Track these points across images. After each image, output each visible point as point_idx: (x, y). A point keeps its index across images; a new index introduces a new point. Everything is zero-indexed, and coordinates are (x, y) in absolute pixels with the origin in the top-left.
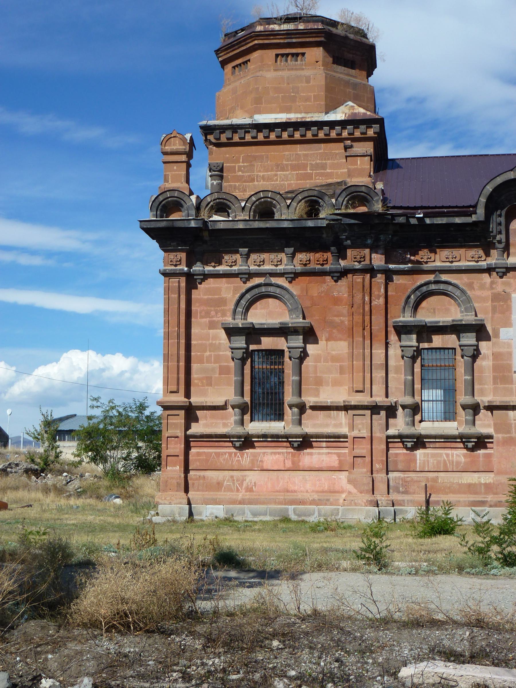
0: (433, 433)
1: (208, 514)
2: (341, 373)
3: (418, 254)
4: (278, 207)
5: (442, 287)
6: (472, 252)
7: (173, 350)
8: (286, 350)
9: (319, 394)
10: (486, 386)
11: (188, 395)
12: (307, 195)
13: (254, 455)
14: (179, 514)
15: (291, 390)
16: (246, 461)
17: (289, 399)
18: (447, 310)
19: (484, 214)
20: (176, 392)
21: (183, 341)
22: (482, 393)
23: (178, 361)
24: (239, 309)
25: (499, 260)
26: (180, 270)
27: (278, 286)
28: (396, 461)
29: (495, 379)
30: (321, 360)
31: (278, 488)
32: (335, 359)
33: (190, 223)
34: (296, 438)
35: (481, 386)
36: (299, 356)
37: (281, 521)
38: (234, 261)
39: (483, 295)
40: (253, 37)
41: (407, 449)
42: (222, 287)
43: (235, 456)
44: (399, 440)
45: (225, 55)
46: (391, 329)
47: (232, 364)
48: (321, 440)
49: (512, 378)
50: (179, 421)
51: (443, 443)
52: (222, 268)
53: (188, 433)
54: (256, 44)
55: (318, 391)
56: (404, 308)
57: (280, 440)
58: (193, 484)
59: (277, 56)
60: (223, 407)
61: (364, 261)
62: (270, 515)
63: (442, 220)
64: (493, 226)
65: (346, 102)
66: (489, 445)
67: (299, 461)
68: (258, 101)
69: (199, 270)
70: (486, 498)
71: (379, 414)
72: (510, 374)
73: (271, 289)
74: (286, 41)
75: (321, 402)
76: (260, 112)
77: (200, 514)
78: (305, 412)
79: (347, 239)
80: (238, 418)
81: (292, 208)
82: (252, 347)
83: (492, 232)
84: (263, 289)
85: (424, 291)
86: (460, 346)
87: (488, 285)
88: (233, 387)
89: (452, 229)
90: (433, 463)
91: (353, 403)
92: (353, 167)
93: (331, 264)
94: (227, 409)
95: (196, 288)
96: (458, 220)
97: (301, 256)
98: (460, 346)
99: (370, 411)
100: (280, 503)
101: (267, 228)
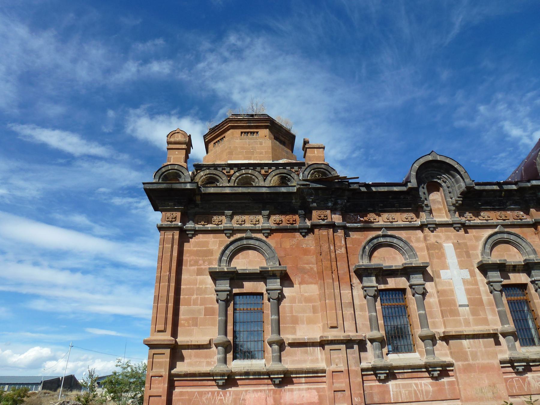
0: (402, 364)
3: (367, 216)
4: (257, 180)
5: (388, 239)
6: (405, 215)
7: (164, 293)
8: (265, 292)
9: (295, 332)
10: (437, 320)
11: (174, 334)
12: (279, 172)
13: (236, 393)
15: (270, 329)
16: (228, 400)
17: (269, 337)
18: (394, 258)
19: (416, 183)
20: (164, 331)
21: (173, 285)
22: (435, 325)
23: (167, 303)
24: (224, 258)
26: (175, 224)
28: (372, 393)
30: (296, 300)
32: (308, 300)
33: (186, 186)
34: (278, 374)
35: (433, 320)
36: (277, 297)
38: (220, 220)
39: (420, 247)
40: (228, 122)
41: (380, 380)
42: (210, 241)
43: (218, 395)
44: (372, 373)
45: (210, 137)
46: (353, 274)
47: (217, 306)
48: (301, 375)
49: (458, 311)
50: (164, 360)
51: (410, 374)
52: (209, 226)
53: (172, 372)
54: (229, 126)
55: (294, 328)
56: (362, 256)
57: (262, 377)
59: (242, 133)
63: (384, 189)
65: (283, 159)
66: (450, 373)
67: (281, 398)
69: (191, 227)
71: (353, 348)
72: (456, 308)
73: (251, 242)
74: (247, 124)
75: (299, 339)
78: (284, 350)
79: (313, 202)
80: (221, 356)
82: (235, 291)
84: (245, 242)
85: (375, 243)
88: (217, 327)
90: (405, 393)
93: (300, 223)
94: (210, 348)
95: (189, 242)
97: (275, 217)
98: (411, 286)
99: (345, 346)
101: (249, 192)
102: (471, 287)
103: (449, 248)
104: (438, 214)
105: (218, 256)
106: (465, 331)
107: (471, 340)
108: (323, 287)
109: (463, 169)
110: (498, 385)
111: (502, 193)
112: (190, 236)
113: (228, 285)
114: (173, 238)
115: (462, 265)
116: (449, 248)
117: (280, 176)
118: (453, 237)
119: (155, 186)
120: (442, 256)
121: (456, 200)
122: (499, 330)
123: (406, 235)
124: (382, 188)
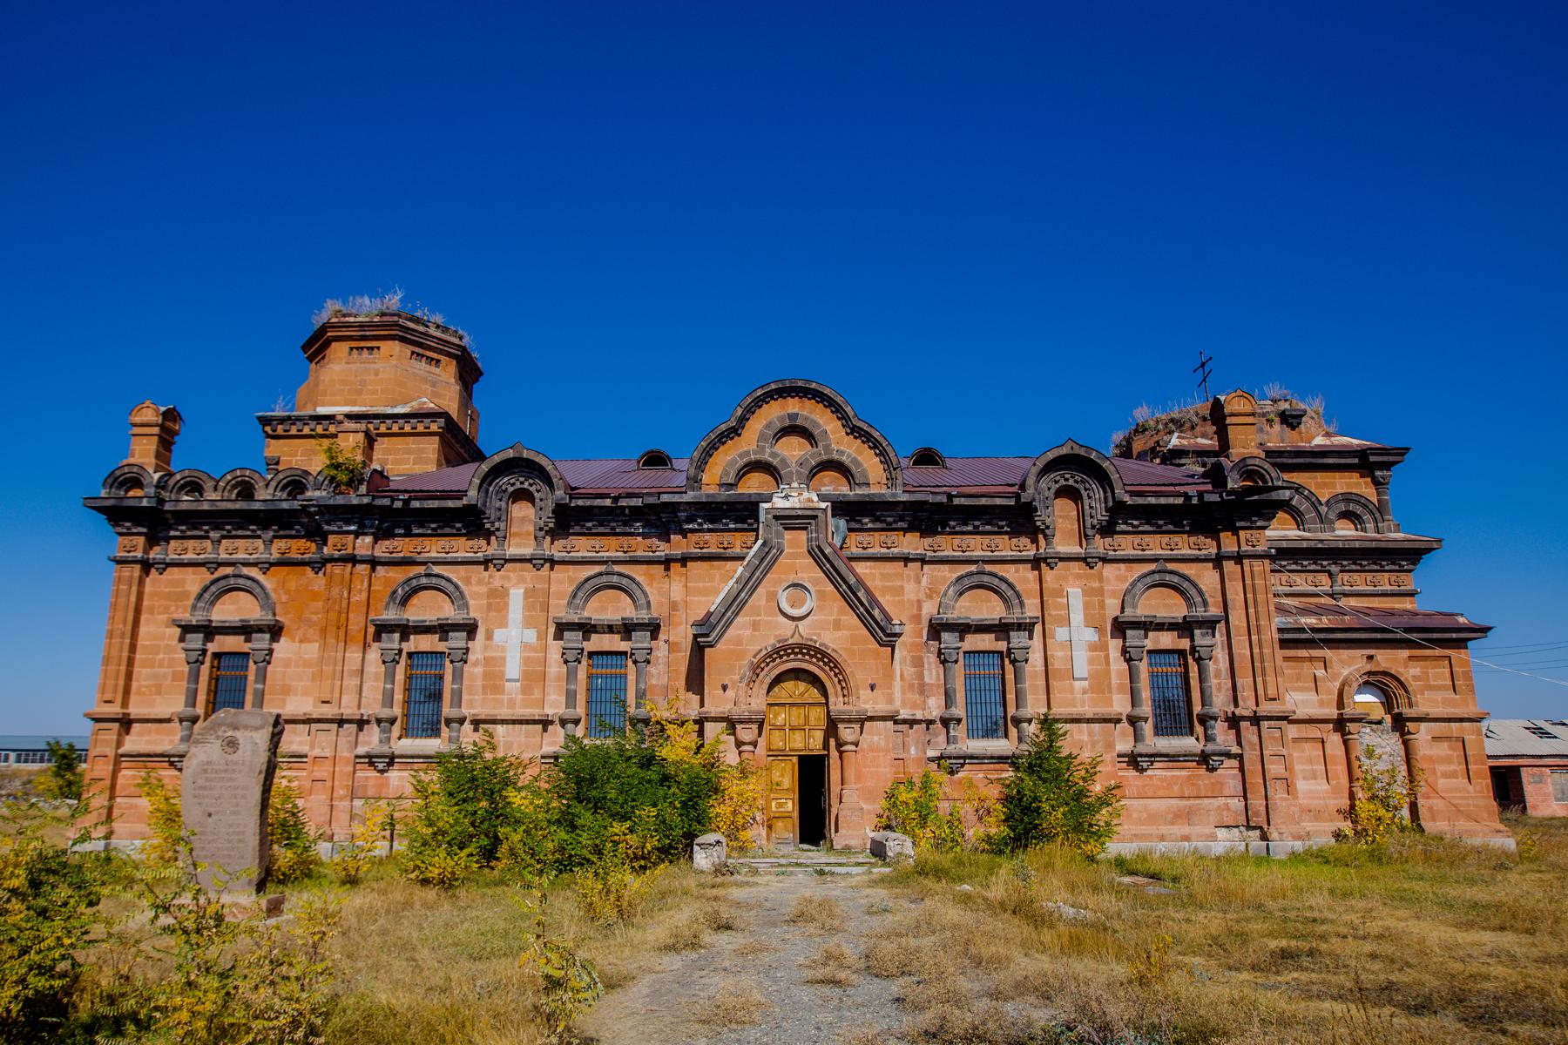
2: (312, 681)
5: (434, 581)
11: (125, 704)
22: (471, 704)
27: (249, 578)
29: (484, 687)
32: (307, 664)
35: (472, 697)
41: (379, 771)
47: (186, 668)
59: (352, 349)
60: (169, 720)
74: (359, 333)
84: (232, 581)
87: (486, 580)
91: (314, 717)
96: (450, 504)
103: (516, 596)
105: (192, 601)
108: (324, 647)
109: (558, 474)
115: (528, 623)
116: (516, 596)
120: (504, 608)
124: (430, 502)
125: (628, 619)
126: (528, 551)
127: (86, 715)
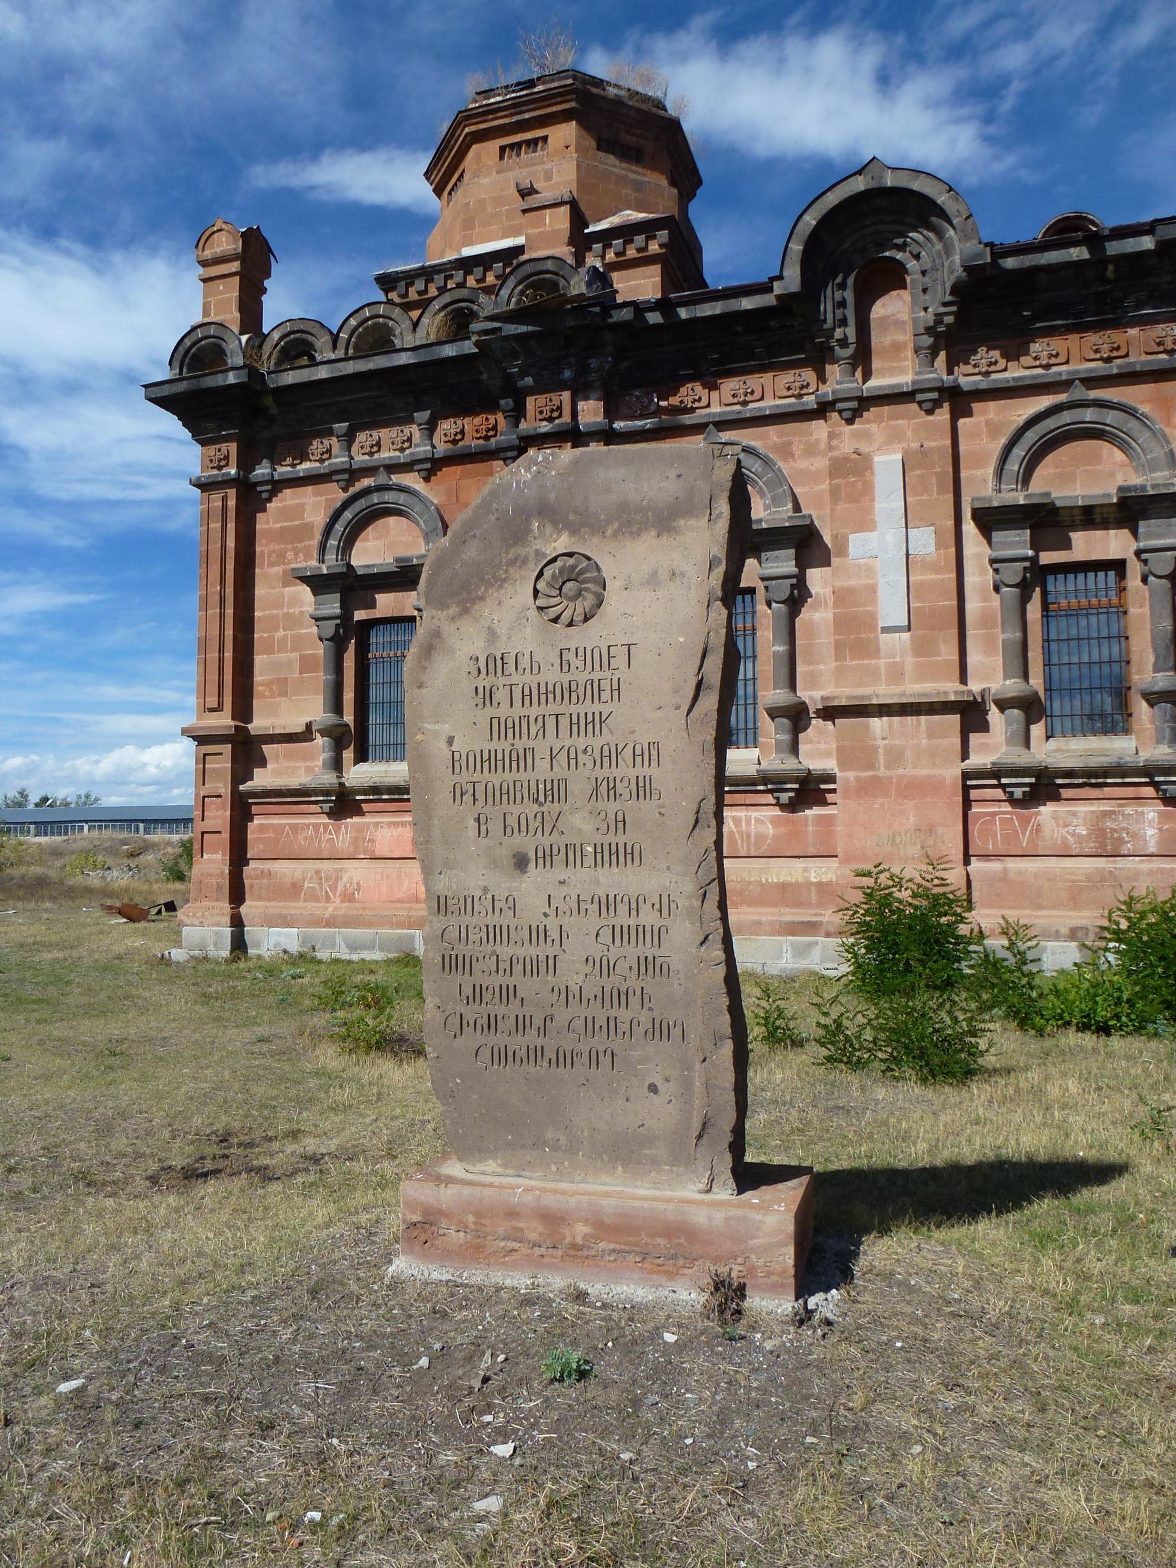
1: (271, 947)
13: (359, 829)
14: (215, 945)
16: (343, 842)
20: (219, 708)
22: (813, 683)
23: (221, 650)
24: (333, 542)
25: (842, 383)
26: (223, 475)
27: (402, 489)
29: (838, 646)
31: (399, 896)
35: (811, 668)
37: (398, 961)
39: (813, 468)
43: (325, 832)
52: (305, 467)
53: (241, 787)
54: (467, 134)
58: (252, 886)
59: (503, 149)
61: (560, 416)
62: (381, 949)
63: (712, 308)
64: (827, 308)
65: (621, 210)
66: (830, 797)
68: (468, 224)
70: (821, 915)
72: (872, 636)
73: (389, 496)
74: (514, 119)
76: (471, 243)
77: (258, 945)
79: (523, 374)
81: (421, 330)
83: (825, 321)
84: (375, 498)
86: (763, 579)
87: (823, 445)
89: (740, 329)
92: (537, 231)
95: (264, 510)
100: (401, 925)
102: (933, 577)
104: (887, 364)
105: (318, 538)
106: (877, 696)
107: (896, 719)
110: (940, 830)
111: (1106, 268)
112: (265, 495)
113: (338, 605)
114: (225, 508)
117: (452, 311)
118: (909, 433)
119: (166, 391)
121: (936, 315)
122: (993, 691)
123: (778, 437)
124: (706, 305)
125: (1135, 488)
126: (904, 379)
127: (186, 732)
